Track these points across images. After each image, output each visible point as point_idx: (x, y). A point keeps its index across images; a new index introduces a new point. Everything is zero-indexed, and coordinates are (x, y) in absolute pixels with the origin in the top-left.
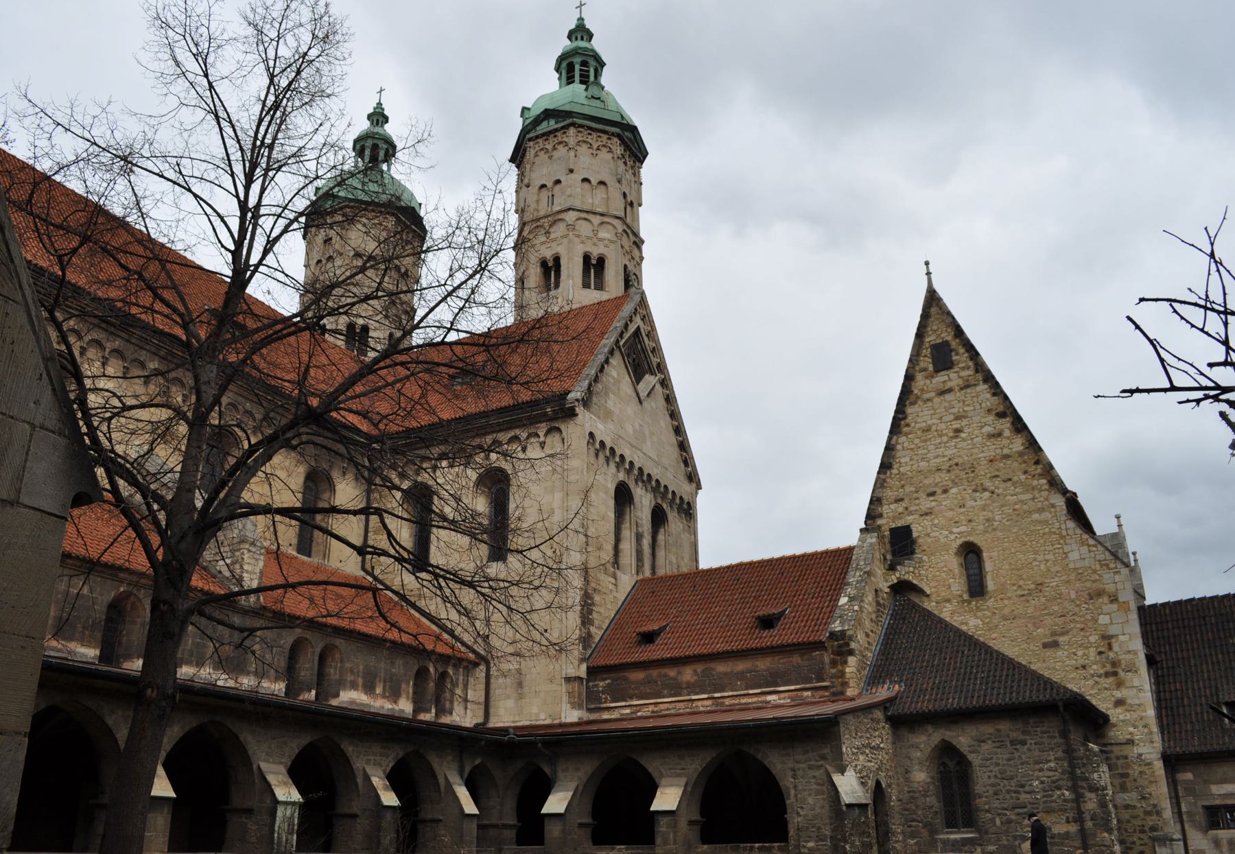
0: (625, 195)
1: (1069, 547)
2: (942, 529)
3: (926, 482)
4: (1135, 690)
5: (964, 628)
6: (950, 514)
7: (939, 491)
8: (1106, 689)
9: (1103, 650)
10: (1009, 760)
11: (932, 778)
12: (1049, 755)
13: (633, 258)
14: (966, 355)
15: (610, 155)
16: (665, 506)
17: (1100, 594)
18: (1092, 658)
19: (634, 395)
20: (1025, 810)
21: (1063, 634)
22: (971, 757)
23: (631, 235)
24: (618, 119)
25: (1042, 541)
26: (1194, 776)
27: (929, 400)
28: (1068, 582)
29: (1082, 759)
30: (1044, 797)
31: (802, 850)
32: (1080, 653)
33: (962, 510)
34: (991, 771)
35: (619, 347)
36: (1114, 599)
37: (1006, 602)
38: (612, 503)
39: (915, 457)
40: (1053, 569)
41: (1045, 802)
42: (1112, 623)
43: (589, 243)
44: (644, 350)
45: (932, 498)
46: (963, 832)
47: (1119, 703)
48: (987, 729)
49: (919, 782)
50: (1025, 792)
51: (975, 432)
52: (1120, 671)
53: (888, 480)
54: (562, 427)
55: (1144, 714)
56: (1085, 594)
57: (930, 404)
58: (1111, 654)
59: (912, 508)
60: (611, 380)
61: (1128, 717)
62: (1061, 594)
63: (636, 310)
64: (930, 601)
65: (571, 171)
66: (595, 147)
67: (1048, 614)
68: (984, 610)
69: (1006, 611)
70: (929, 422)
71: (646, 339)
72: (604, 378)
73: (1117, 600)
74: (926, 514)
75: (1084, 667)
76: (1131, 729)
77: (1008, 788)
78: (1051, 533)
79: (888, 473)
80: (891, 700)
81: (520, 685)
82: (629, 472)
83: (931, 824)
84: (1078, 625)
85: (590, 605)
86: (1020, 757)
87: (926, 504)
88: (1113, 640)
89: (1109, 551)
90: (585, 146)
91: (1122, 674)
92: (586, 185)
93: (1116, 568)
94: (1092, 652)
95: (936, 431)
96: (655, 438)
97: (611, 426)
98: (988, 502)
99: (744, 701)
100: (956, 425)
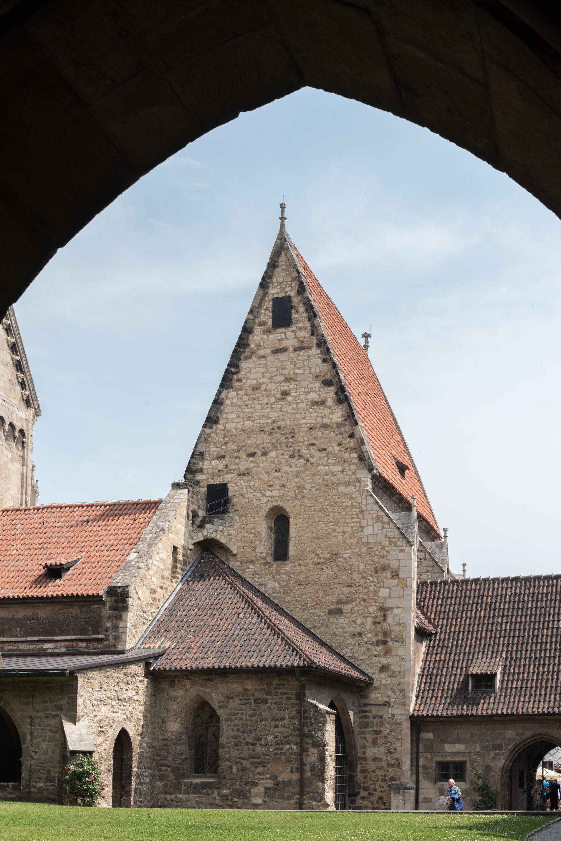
2: (256, 491)
3: (249, 442)
6: (265, 477)
7: (259, 453)
10: (251, 716)
11: (187, 728)
14: (305, 315)
18: (368, 627)
20: (259, 760)
21: (348, 602)
22: (219, 712)
27: (263, 357)
28: (360, 555)
29: (311, 718)
32: (359, 622)
33: (277, 474)
34: (235, 725)
37: (303, 568)
39: (241, 415)
40: (349, 542)
42: (390, 597)
45: (251, 459)
46: (207, 777)
47: (384, 669)
48: (236, 687)
49: (172, 732)
50: (260, 745)
51: (302, 397)
52: (389, 640)
53: (213, 435)
56: (372, 568)
57: (263, 361)
58: (385, 625)
59: (232, 467)
61: (389, 682)
62: (351, 566)
69: (302, 577)
70: (260, 380)
74: (244, 474)
75: (360, 635)
76: (390, 693)
77: (248, 740)
79: (214, 427)
83: (178, 769)
84: (362, 596)
86: (261, 714)
87: (246, 464)
94: (369, 621)
95: (265, 390)
99: (21, 647)
100: (285, 387)
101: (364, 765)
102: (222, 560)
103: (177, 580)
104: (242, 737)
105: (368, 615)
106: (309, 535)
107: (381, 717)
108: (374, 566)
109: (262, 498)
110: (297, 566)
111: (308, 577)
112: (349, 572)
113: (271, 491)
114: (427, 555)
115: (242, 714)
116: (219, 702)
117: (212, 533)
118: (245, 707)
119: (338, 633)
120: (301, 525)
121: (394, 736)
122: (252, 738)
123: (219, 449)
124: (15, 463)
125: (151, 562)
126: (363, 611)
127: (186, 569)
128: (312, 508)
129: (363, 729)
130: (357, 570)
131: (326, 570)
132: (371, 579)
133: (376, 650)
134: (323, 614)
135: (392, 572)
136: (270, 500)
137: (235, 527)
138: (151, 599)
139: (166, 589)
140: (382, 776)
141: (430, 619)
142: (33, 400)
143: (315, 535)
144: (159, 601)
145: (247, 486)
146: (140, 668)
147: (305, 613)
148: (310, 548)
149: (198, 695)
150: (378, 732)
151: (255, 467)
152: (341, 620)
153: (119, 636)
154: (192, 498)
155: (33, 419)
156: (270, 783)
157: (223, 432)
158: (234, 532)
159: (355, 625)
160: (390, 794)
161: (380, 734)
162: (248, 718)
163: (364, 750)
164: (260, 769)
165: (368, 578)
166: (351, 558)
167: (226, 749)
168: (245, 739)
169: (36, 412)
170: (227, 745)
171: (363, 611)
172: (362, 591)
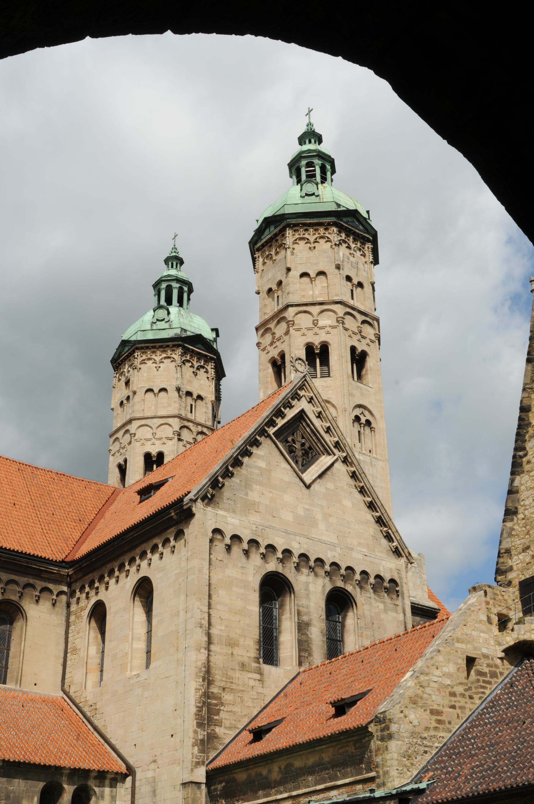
0: (349, 279)
13: (363, 337)
15: (329, 244)
16: (349, 588)
24: (333, 208)
35: (269, 436)
38: (255, 597)
43: (311, 333)
54: (185, 531)
60: (257, 471)
63: (297, 393)
65: (289, 270)
66: (312, 239)
72: (240, 473)
81: (154, 791)
82: (281, 561)
85: (216, 705)
90: (302, 243)
92: (306, 279)
96: (333, 520)
97: (255, 518)
103: (481, 695)
124: (390, 613)
125: (427, 678)
127: (496, 682)
139: (461, 708)
142: (403, 550)
144: (450, 723)
153: (388, 771)
155: (407, 567)
169: (408, 560)
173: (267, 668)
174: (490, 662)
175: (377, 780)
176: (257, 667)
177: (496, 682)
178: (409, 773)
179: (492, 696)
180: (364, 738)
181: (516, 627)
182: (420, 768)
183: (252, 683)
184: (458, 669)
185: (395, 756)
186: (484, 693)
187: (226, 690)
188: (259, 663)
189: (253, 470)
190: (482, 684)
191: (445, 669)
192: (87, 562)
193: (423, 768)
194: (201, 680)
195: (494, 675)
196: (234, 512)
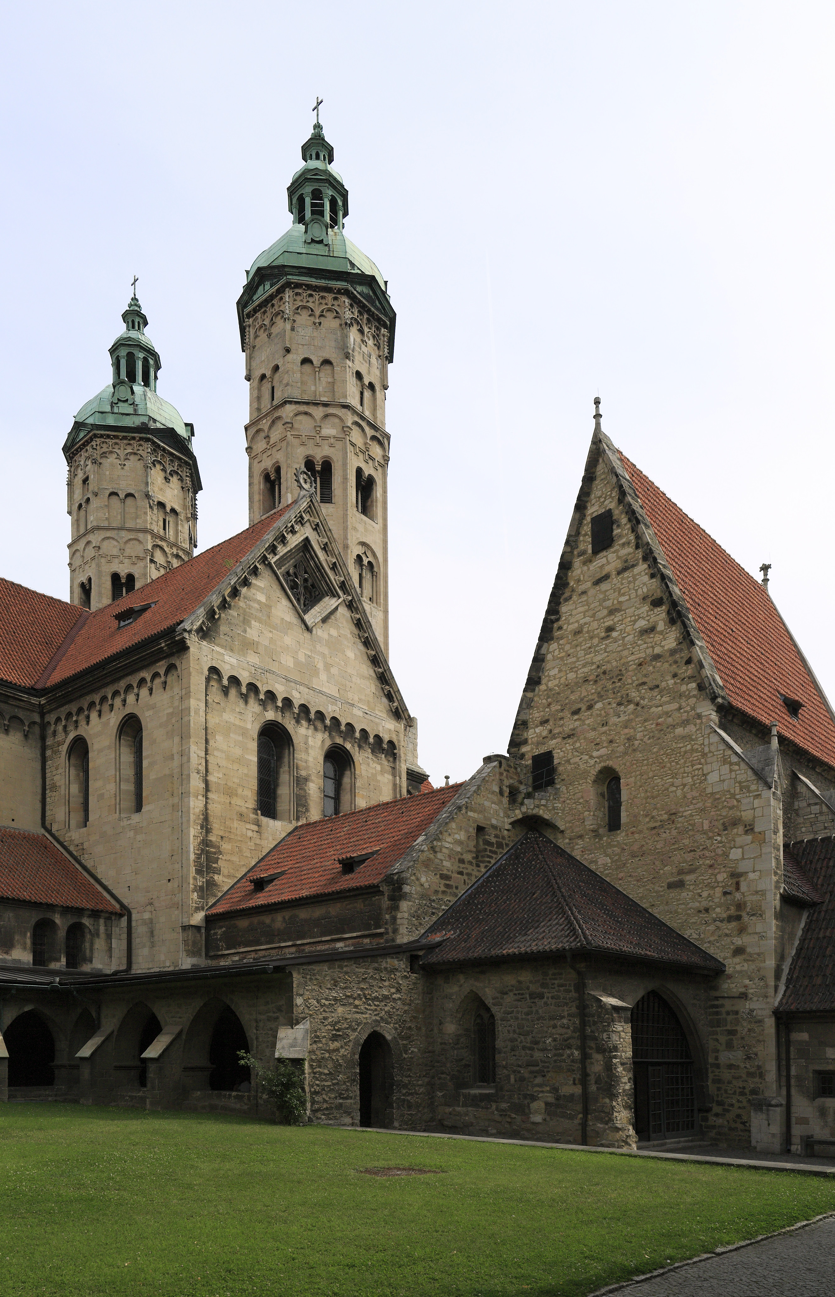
1: (709, 766)
2: (582, 754)
4: (756, 937)
5: (593, 867)
6: (592, 735)
8: (727, 935)
9: (728, 889)
10: (527, 1014)
12: (563, 1011)
17: (735, 823)
18: (717, 900)
19: (299, 621)
20: (537, 1068)
22: (494, 1009)
23: (367, 429)
25: (682, 761)
26: (810, 1037)
30: (555, 1055)
31: (259, 1101)
32: (705, 894)
33: (605, 728)
34: (510, 1026)
36: (749, 829)
37: (637, 836)
41: (555, 1061)
44: (319, 567)
45: (576, 717)
48: (510, 980)
50: (538, 1049)
52: (744, 914)
53: (536, 699)
55: (762, 965)
56: (719, 825)
58: (738, 896)
59: (556, 731)
64: (564, 838)
67: (678, 849)
68: (615, 846)
71: (321, 555)
73: (752, 829)
74: (569, 736)
75: (707, 910)
76: (747, 982)
77: (524, 1044)
78: (692, 750)
80: (432, 948)
84: (708, 862)
86: (537, 1011)
87: (570, 724)
88: (742, 879)
89: (752, 769)
91: (746, 918)
93: (757, 790)
94: (718, 892)
98: (632, 716)
101: (717, 1074)
102: (549, 840)
104: (519, 1040)
105: (716, 884)
106: (643, 795)
107: (737, 1013)
108: (721, 821)
109: (589, 760)
110: (630, 835)
111: (643, 846)
112: (691, 833)
113: (598, 750)
114: (824, 807)
115: (518, 1012)
116: (493, 999)
117: (532, 809)
118: (520, 1003)
119: (679, 910)
120: (633, 785)
121: (754, 1037)
122: (529, 1040)
123: (542, 713)
125: (439, 844)
126: (709, 881)
128: (645, 762)
129: (714, 1029)
130: (701, 829)
131: (664, 835)
132: (719, 838)
133: (727, 928)
134: (661, 889)
135: (746, 827)
136: (598, 760)
137: (561, 799)
138: (442, 886)
139: (468, 874)
140: (740, 1088)
141: (817, 885)
143: (649, 794)
144: (457, 888)
145: (572, 749)
146: (401, 962)
147: (641, 890)
148: (644, 811)
149: (472, 991)
150: (732, 1033)
151: (580, 726)
152: (683, 894)
154: (508, 771)
156: (550, 1098)
157: (546, 693)
158: (560, 805)
159: (700, 899)
160: (750, 1112)
161: (734, 1035)
162: (524, 1017)
163: (717, 1054)
164: (539, 1080)
165: (715, 838)
166: (693, 816)
167: (502, 1055)
168: (521, 1042)
170: (504, 1050)
171: (709, 881)
172: (707, 855)
173: (265, 820)
174: (498, 832)
175: (385, 937)
176: (255, 819)
177: (501, 853)
178: (418, 932)
179: (497, 865)
180: (374, 897)
181: (526, 801)
182: (427, 928)
183: (250, 834)
184: (469, 837)
185: (406, 915)
186: (489, 862)
187: (224, 839)
188: (257, 815)
189: (251, 603)
190: (488, 853)
191: (457, 837)
192: (61, 691)
193: (430, 928)
194: (199, 828)
195: (500, 845)
196: (232, 650)
